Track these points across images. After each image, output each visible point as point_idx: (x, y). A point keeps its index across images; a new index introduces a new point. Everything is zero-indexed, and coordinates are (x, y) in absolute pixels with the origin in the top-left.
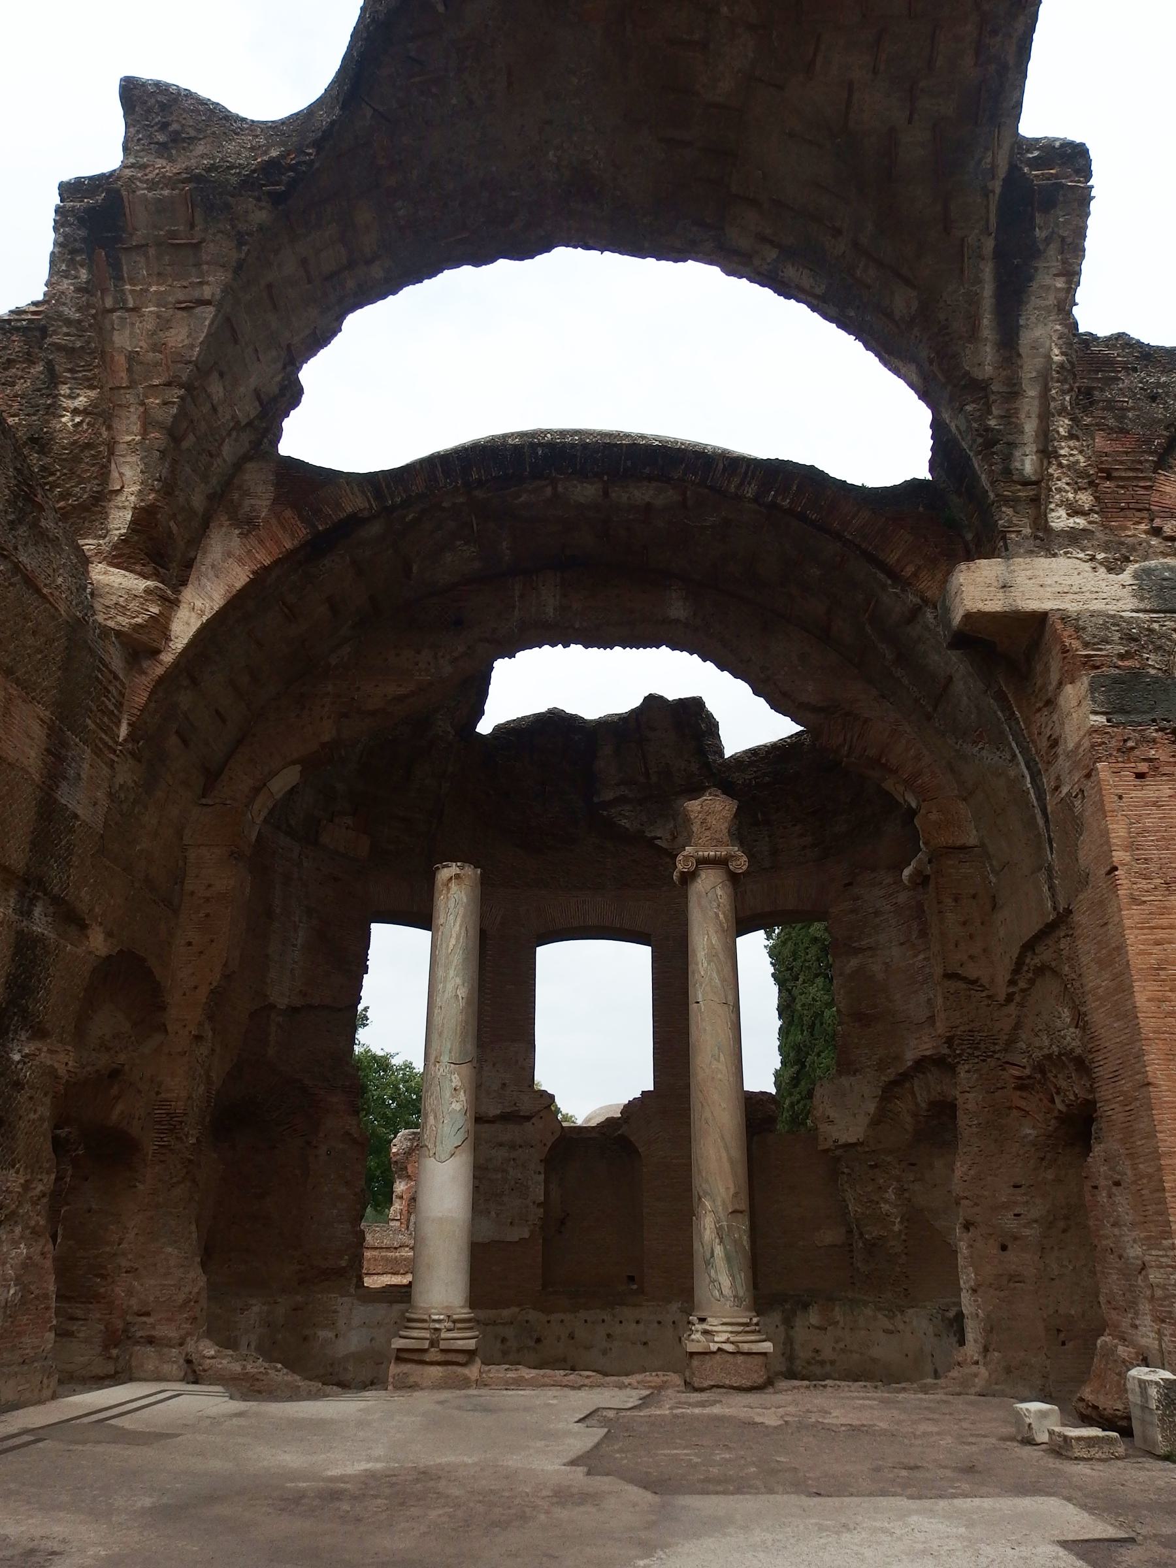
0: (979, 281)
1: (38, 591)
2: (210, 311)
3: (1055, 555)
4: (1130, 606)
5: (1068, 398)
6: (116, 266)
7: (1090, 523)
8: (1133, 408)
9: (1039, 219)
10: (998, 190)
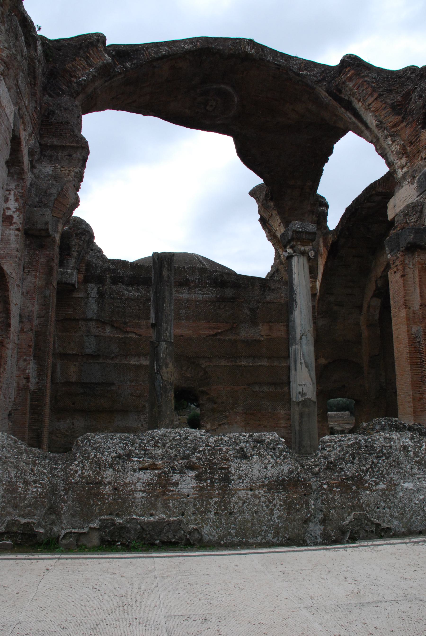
0: (350, 119)
1: (273, 303)
2: (282, 224)
3: (403, 187)
4: (416, 196)
5: (385, 131)
6: (269, 225)
7: (408, 167)
8: (415, 108)
9: (343, 96)
10: (331, 98)
